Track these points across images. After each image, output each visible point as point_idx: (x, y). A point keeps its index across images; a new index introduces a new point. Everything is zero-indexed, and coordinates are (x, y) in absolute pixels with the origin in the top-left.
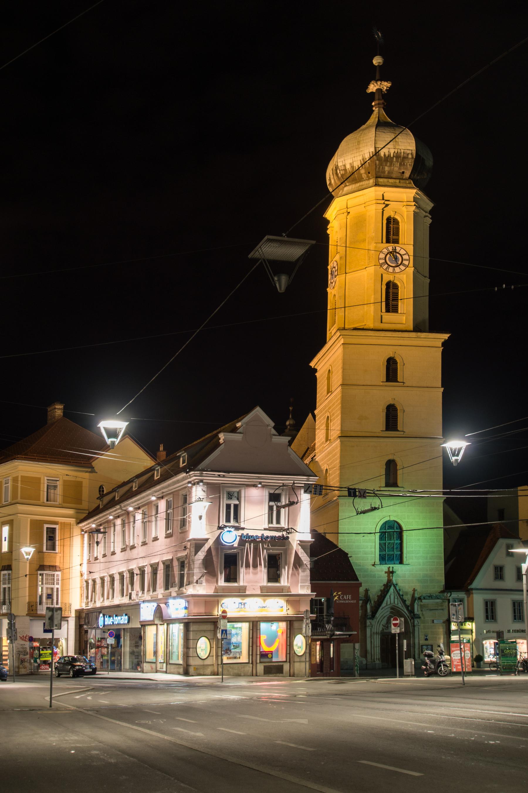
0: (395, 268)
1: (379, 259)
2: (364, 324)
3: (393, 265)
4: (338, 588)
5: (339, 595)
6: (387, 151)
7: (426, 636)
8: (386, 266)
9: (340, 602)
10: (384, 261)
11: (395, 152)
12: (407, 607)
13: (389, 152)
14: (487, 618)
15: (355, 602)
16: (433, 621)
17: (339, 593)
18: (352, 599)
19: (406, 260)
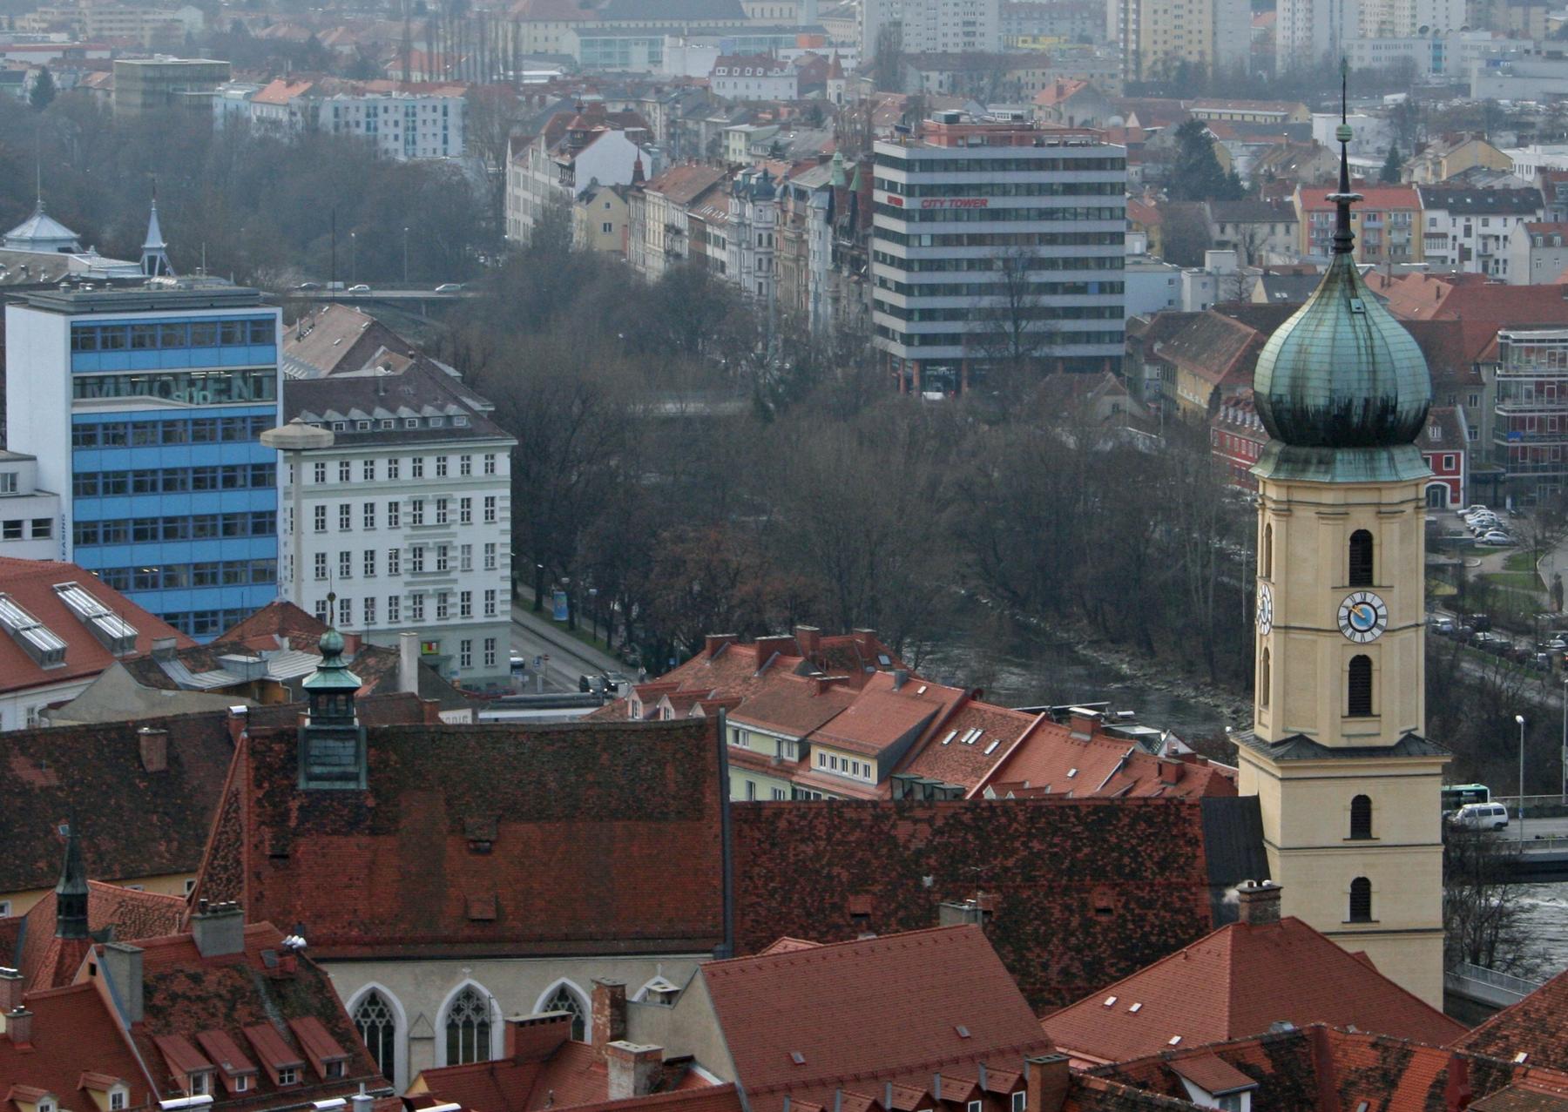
2: (1313, 731)
8: (1351, 630)
10: (1346, 622)
19: (1383, 617)
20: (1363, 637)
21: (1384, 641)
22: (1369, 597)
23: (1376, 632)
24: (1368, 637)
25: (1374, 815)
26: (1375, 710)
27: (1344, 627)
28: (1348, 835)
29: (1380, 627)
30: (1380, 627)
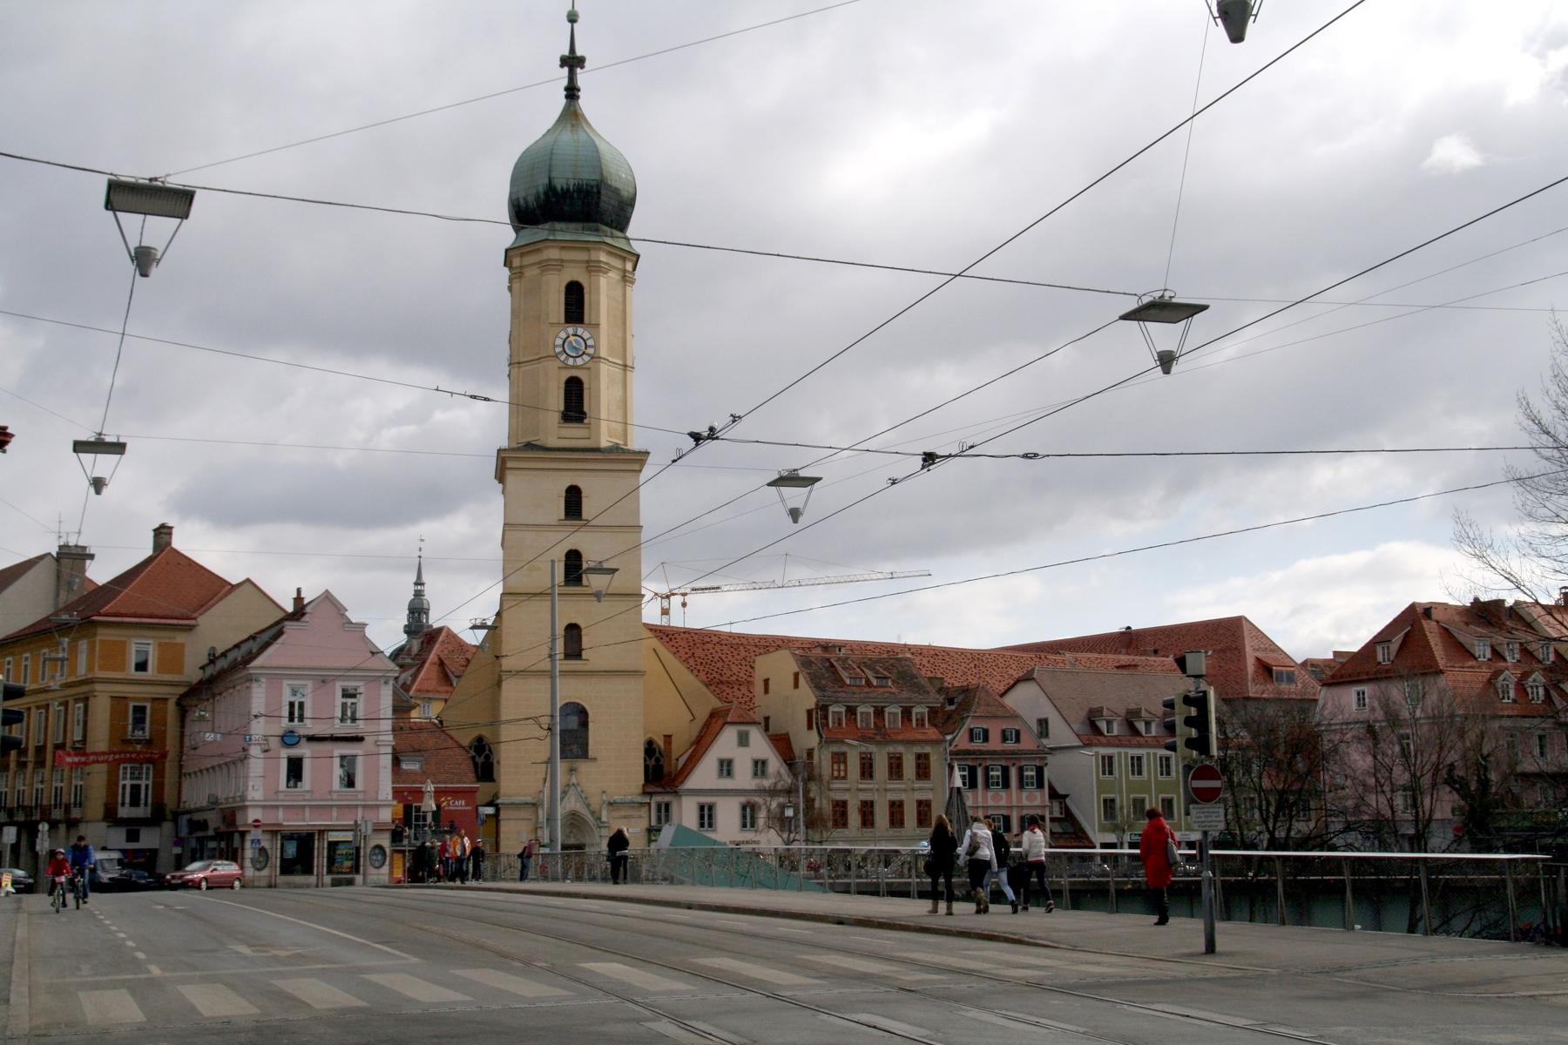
0: (577, 359)
2: (538, 438)
3: (574, 355)
5: (449, 801)
8: (565, 355)
10: (561, 349)
12: (593, 813)
14: (744, 825)
18: (467, 805)
19: (591, 347)
20: (575, 361)
22: (580, 331)
23: (586, 358)
24: (579, 361)
25: (584, 501)
27: (560, 353)
28: (563, 517)
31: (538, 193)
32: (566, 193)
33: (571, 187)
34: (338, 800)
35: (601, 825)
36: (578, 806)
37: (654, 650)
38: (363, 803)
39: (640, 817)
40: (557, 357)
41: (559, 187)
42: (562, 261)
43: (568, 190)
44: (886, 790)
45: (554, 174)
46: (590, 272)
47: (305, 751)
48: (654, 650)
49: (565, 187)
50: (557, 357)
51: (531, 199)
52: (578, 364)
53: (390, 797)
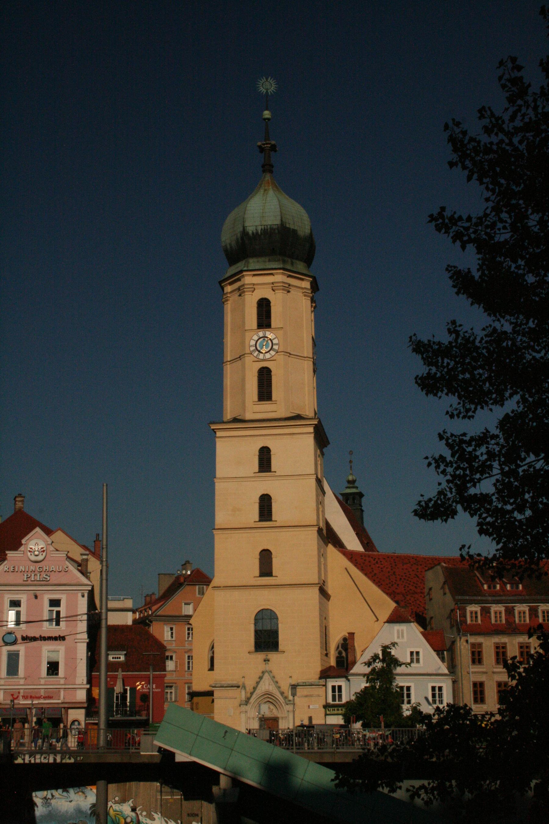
1: (250, 346)
4: (141, 678)
5: (143, 685)
6: (255, 229)
7: (302, 721)
8: (257, 352)
9: (144, 690)
10: (254, 348)
11: (262, 229)
12: (282, 693)
13: (256, 230)
15: (160, 690)
16: (309, 706)
17: (143, 683)
19: (276, 344)
21: (277, 357)
23: (272, 353)
24: (268, 356)
26: (273, 398)
27: (253, 351)
28: (257, 470)
29: (274, 350)
30: (274, 350)
31: (237, 239)
32: (256, 236)
33: (259, 231)
34: (45, 685)
35: (288, 703)
36: (272, 689)
37: (346, 569)
38: (63, 687)
39: (319, 696)
40: (251, 354)
41: (250, 232)
42: (254, 284)
43: (257, 233)
44: (494, 673)
45: (247, 224)
46: (274, 291)
47: (21, 648)
48: (346, 569)
49: (255, 231)
50: (251, 354)
51: (234, 244)
52: (267, 358)
53: (85, 682)
